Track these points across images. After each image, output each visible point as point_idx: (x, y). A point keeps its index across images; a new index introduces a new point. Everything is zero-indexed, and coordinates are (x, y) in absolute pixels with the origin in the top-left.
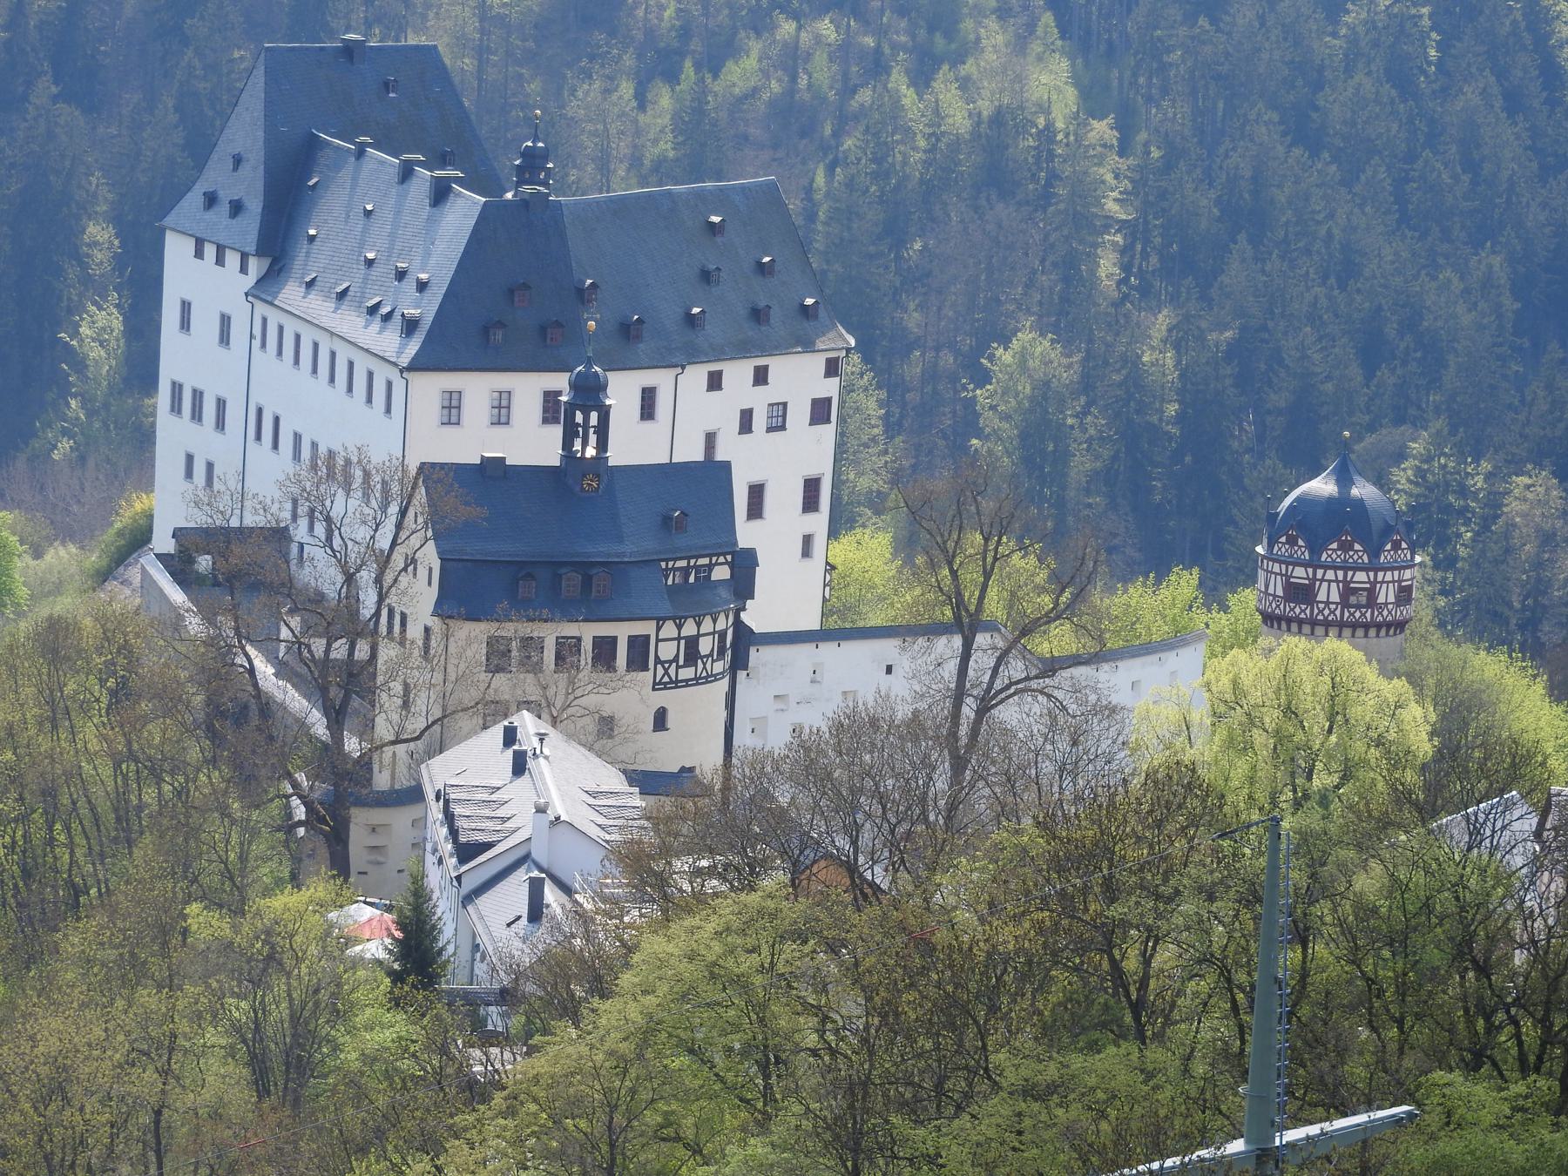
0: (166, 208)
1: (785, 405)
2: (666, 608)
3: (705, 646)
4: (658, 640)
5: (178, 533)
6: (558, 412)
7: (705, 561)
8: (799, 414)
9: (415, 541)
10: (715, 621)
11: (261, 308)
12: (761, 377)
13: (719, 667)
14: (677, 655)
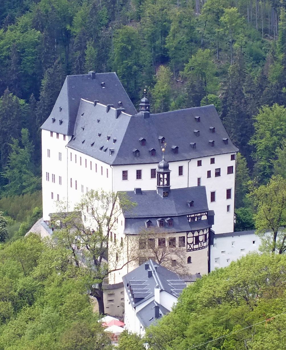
0: (42, 122)
1: (220, 169)
2: (188, 228)
3: (201, 238)
4: (187, 238)
5: (50, 215)
6: (155, 174)
7: (200, 215)
8: (224, 171)
9: (118, 213)
10: (203, 231)
11: (70, 150)
12: (213, 161)
13: (205, 244)
14: (193, 242)
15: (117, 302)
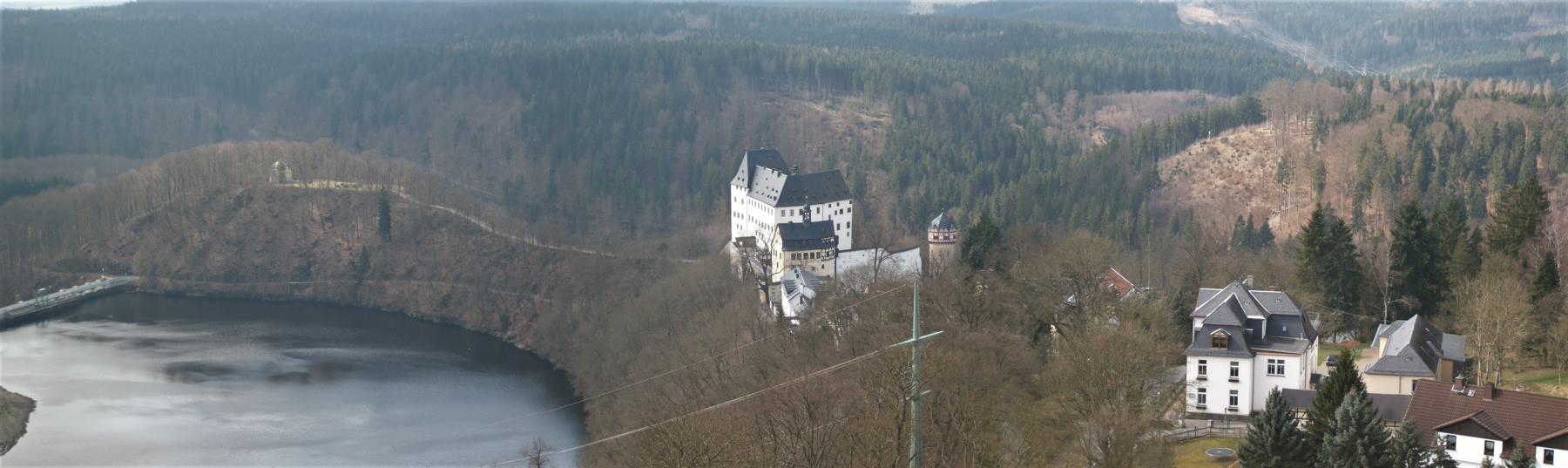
5: (736, 239)
12: (838, 205)
15: (777, 294)
